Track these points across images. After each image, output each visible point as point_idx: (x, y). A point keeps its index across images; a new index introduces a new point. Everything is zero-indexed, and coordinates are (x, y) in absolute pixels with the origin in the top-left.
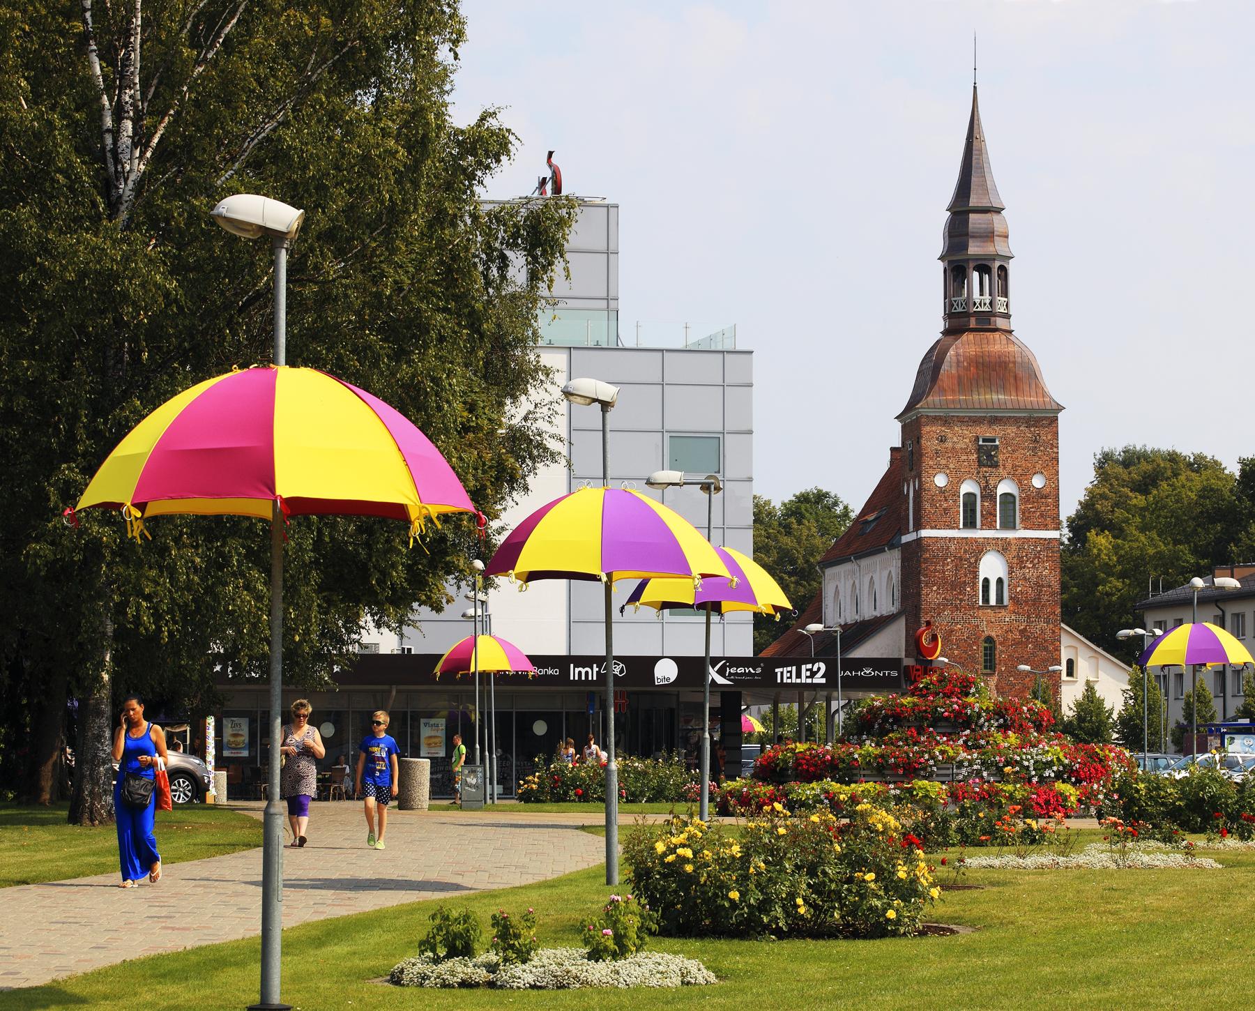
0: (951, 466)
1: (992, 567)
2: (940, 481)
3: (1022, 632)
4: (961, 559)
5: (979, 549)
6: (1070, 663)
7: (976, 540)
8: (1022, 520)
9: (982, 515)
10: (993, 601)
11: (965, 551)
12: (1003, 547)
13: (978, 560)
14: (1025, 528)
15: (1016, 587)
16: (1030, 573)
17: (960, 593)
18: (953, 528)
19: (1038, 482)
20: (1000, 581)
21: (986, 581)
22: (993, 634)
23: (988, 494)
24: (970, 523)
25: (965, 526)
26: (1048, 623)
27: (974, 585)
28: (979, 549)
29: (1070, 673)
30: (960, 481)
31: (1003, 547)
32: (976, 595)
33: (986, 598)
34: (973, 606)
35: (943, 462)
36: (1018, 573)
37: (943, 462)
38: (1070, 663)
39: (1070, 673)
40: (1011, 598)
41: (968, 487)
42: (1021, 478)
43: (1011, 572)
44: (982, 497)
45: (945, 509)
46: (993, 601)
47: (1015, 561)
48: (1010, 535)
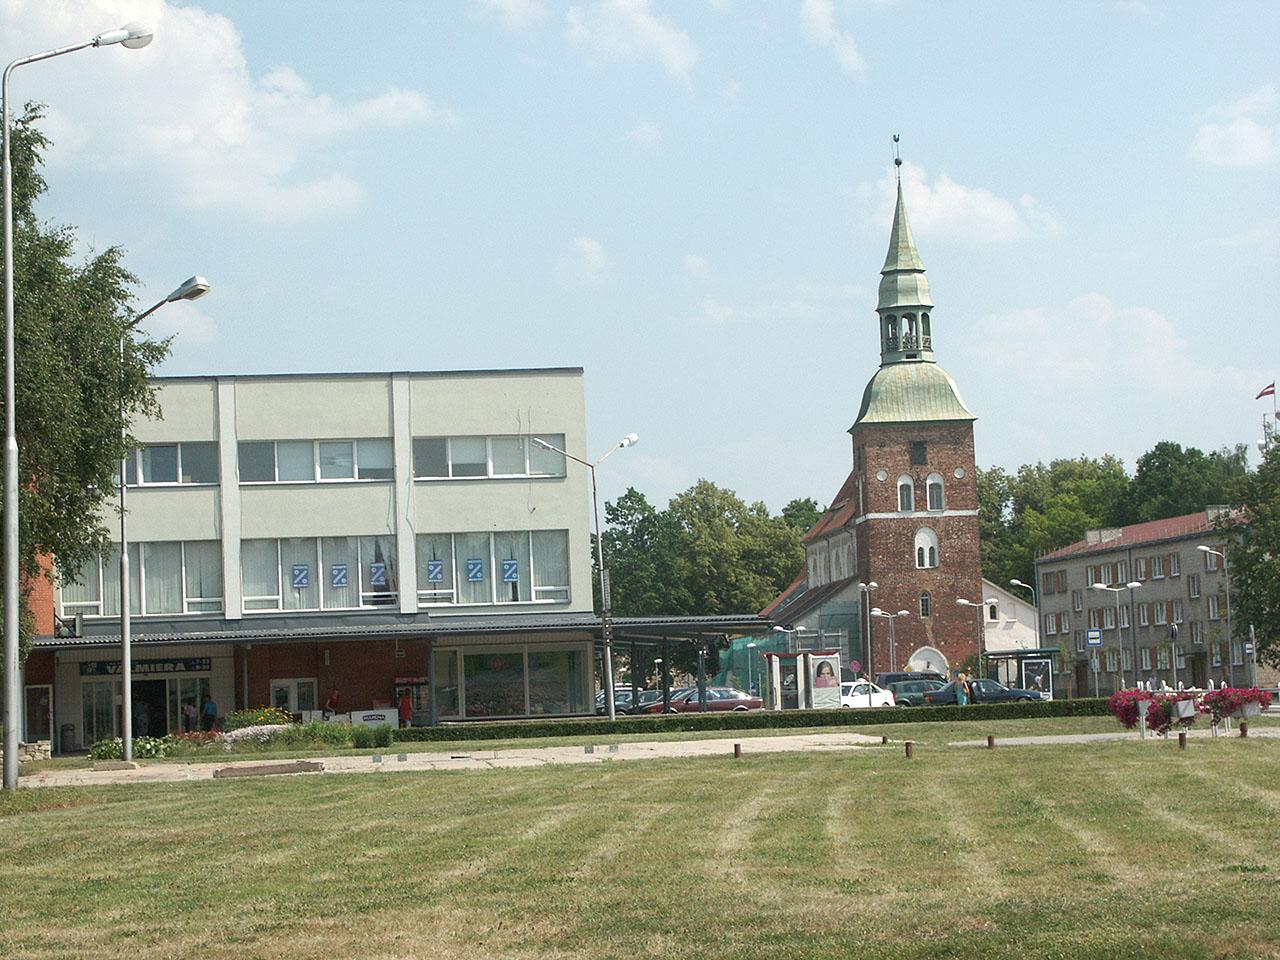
1: (924, 540)
10: (927, 565)
12: (933, 523)
13: (913, 535)
14: (951, 509)
15: (945, 553)
16: (956, 542)
23: (920, 485)
24: (906, 507)
26: (971, 579)
28: (914, 526)
29: (993, 615)
30: (897, 476)
31: (933, 523)
33: (921, 563)
34: (912, 569)
36: (946, 543)
39: (993, 615)
43: (940, 540)
46: (927, 565)
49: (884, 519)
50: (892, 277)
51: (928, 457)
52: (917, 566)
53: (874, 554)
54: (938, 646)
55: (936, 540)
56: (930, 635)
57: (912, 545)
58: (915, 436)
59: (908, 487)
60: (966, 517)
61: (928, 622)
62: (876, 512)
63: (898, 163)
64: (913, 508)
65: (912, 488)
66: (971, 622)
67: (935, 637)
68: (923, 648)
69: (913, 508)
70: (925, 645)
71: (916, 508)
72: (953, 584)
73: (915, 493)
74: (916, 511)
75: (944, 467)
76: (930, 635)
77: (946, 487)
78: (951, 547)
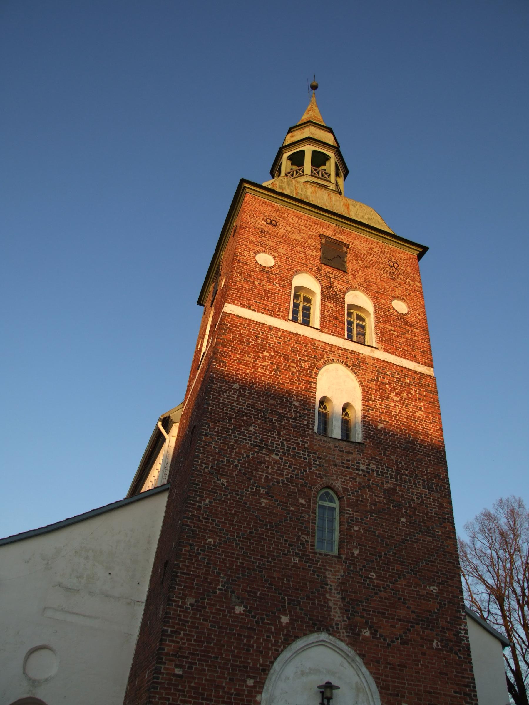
2: (266, 260)
4: (286, 358)
7: (312, 341)
9: (322, 315)
11: (294, 350)
12: (356, 363)
14: (386, 350)
18: (277, 316)
22: (338, 484)
25: (295, 319)
26: (431, 490)
37: (270, 243)
41: (305, 280)
43: (366, 399)
45: (267, 292)
47: (373, 385)
49: (258, 323)
51: (349, 266)
54: (354, 641)
56: (334, 600)
58: (330, 229)
62: (243, 306)
66: (434, 589)
67: (350, 606)
68: (313, 637)
70: (319, 630)
72: (394, 489)
73: (323, 305)
76: (334, 600)
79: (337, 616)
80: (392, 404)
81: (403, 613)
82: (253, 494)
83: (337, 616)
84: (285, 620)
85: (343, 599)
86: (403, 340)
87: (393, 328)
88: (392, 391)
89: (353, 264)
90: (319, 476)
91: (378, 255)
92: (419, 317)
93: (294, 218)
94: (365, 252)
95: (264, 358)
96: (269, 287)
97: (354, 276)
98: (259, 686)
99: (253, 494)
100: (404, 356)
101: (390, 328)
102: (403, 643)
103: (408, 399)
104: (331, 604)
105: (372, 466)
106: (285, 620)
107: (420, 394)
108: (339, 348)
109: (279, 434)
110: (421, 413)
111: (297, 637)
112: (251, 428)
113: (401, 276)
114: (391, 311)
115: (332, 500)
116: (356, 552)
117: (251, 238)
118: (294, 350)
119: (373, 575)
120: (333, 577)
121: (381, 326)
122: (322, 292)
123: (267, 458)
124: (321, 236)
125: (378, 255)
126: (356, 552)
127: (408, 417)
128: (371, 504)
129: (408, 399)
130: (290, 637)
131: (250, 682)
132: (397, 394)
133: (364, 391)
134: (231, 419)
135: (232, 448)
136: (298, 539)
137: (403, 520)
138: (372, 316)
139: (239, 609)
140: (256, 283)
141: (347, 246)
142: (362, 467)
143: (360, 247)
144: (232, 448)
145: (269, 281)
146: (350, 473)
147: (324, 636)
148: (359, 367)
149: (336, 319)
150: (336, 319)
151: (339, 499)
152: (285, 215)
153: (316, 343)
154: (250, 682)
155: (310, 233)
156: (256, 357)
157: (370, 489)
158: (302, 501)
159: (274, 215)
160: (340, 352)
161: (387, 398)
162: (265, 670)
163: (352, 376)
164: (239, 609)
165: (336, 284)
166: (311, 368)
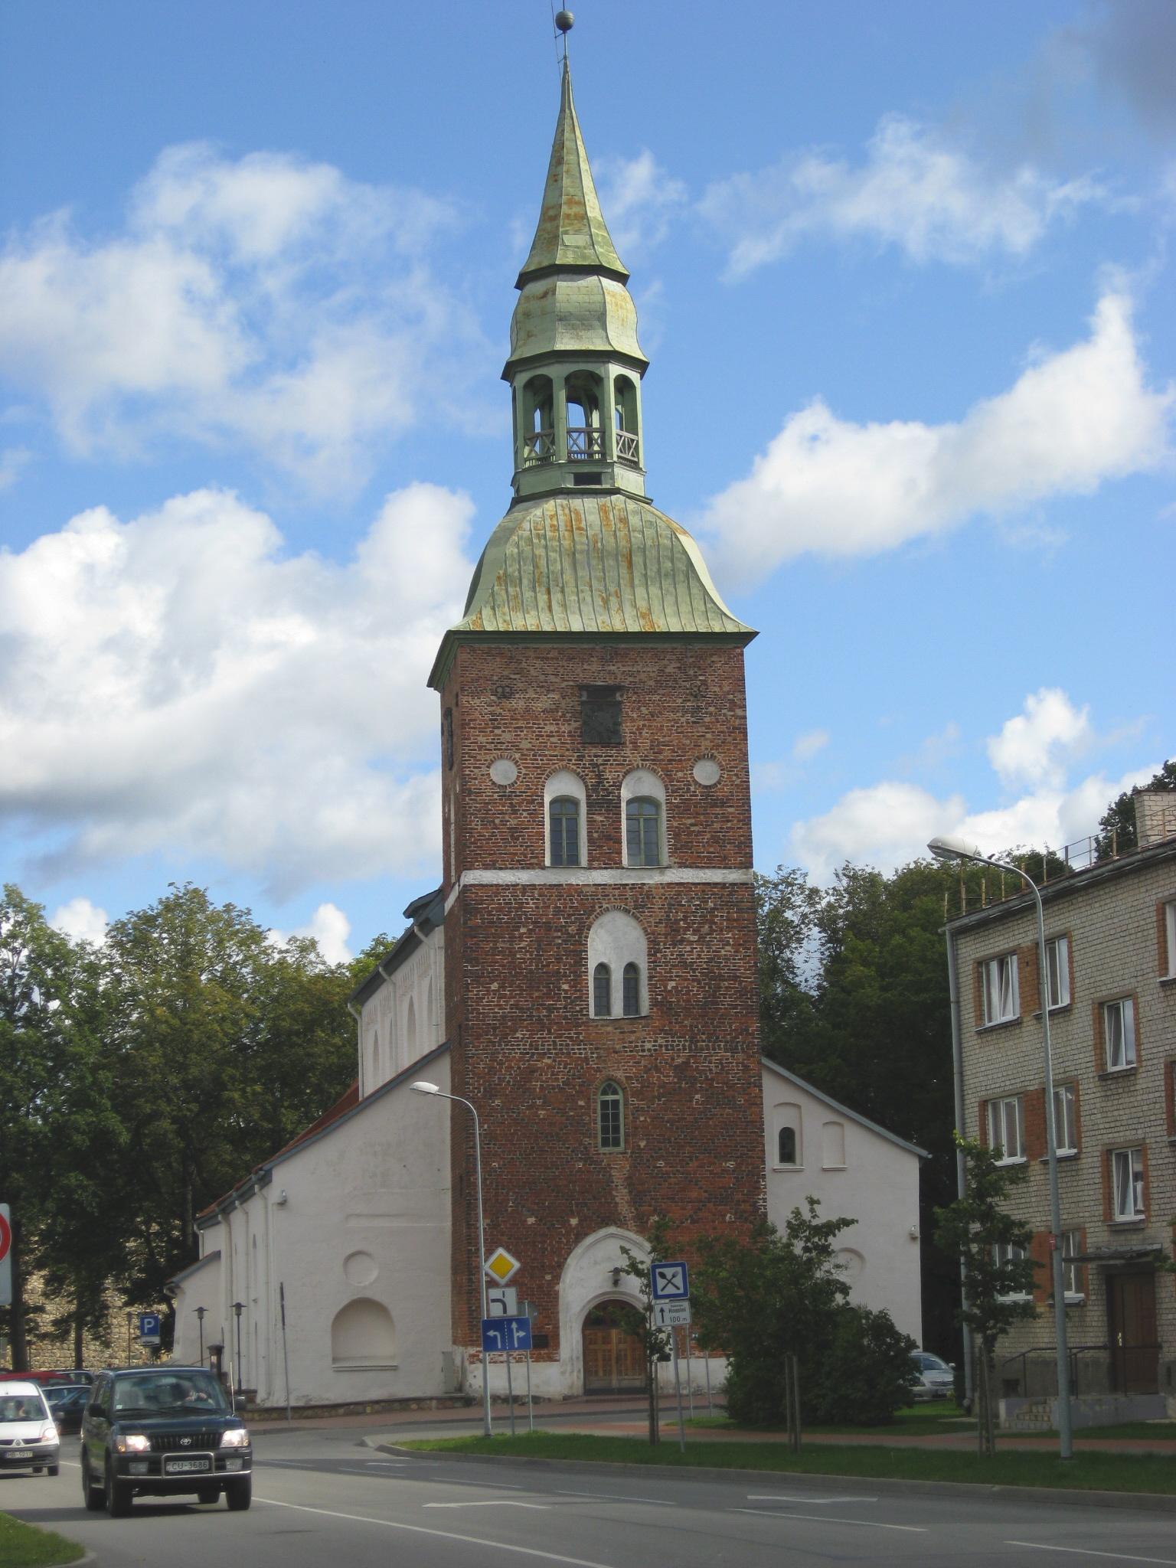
0: (525, 745)
1: (613, 943)
2: (503, 772)
3: (682, 1070)
4: (548, 926)
5: (586, 907)
6: (787, 1137)
7: (577, 890)
8: (674, 851)
9: (591, 840)
10: (617, 1009)
11: (558, 911)
13: (584, 929)
15: (665, 981)
17: (548, 996)
19: (705, 773)
20: (631, 968)
21: (603, 968)
22: (620, 1075)
23: (603, 800)
24: (565, 857)
25: (557, 862)
26: (734, 1050)
27: (578, 981)
28: (586, 907)
29: (788, 1154)
30: (544, 773)
32: (583, 998)
33: (604, 1005)
34: (577, 1019)
35: (507, 737)
36: (669, 953)
37: (507, 737)
38: (787, 1137)
39: (788, 1154)
40: (654, 1003)
41: (563, 785)
42: (669, 768)
43: (653, 952)
44: (589, 805)
46: (617, 1009)
47: (662, 929)
48: (653, 878)
50: (536, 287)
51: (627, 728)
52: (592, 1015)
53: (477, 978)
55: (643, 945)
56: (622, 1196)
57: (579, 956)
58: (594, 671)
59: (573, 802)
60: (723, 885)
61: (618, 1163)
63: (564, 24)
64: (584, 860)
65: (583, 809)
66: (731, 1164)
67: (637, 1197)
68: (602, 1232)
69: (584, 860)
70: (607, 1225)
71: (591, 859)
72: (686, 1063)
73: (591, 822)
74: (590, 868)
75: (667, 754)
76: (622, 1196)
77: (671, 807)
78: (684, 965)
79: (625, 1209)
80: (688, 948)
81: (694, 1195)
82: (529, 1108)
83: (625, 1209)
84: (574, 1222)
85: (630, 1192)
86: (708, 836)
87: (693, 821)
88: (687, 929)
89: (633, 720)
90: (598, 1070)
91: (675, 680)
92: (738, 782)
93: (539, 663)
94: (652, 683)
95: (521, 936)
96: (513, 822)
97: (636, 748)
98: (557, 1278)
99: (529, 1108)
100: (710, 864)
101: (689, 821)
102: (693, 1222)
103: (711, 931)
104: (617, 1199)
105: (660, 1041)
106: (574, 1222)
107: (728, 920)
108: (616, 887)
109: (549, 1032)
110: (728, 948)
111: (587, 1235)
112: (518, 1035)
113: (712, 709)
114: (692, 788)
115: (615, 1092)
116: (642, 1144)
117: (482, 739)
118: (558, 911)
119: (661, 1163)
120: (618, 1176)
121: (675, 824)
122: (588, 796)
123: (539, 1064)
124: (581, 688)
125: (675, 680)
126: (642, 1144)
127: (711, 960)
128: (660, 1087)
129: (711, 931)
130: (580, 1235)
131: (548, 1277)
132: (696, 931)
133: (650, 942)
134: (495, 1029)
135: (501, 1063)
136: (581, 1144)
137: (697, 1096)
138: (664, 807)
139: (531, 1220)
140: (497, 821)
141: (619, 688)
142: (648, 1046)
143: (643, 676)
144: (501, 1063)
145: (515, 812)
146: (634, 1057)
147: (612, 1230)
148: (643, 907)
149: (609, 838)
150: (609, 838)
151: (624, 1089)
152: (524, 665)
153: (585, 890)
154: (548, 1277)
155: (563, 685)
156: (512, 938)
157: (657, 1070)
158: (581, 1103)
159: (505, 673)
160: (617, 892)
161: (682, 941)
162: (561, 1266)
163: (633, 922)
164: (531, 1220)
165: (607, 775)
166: (580, 931)
